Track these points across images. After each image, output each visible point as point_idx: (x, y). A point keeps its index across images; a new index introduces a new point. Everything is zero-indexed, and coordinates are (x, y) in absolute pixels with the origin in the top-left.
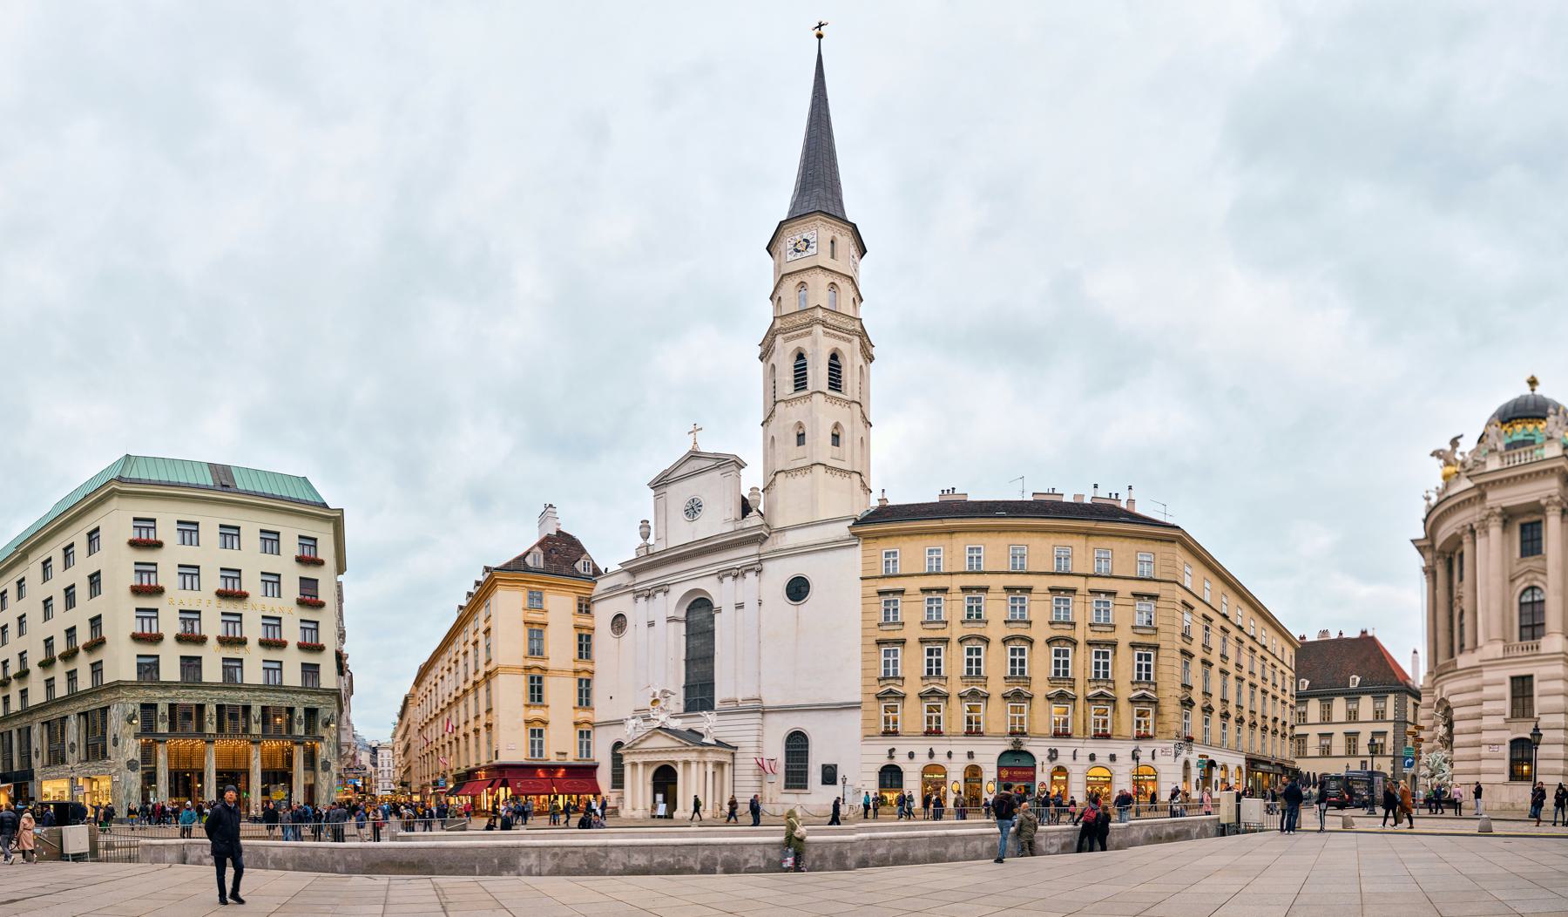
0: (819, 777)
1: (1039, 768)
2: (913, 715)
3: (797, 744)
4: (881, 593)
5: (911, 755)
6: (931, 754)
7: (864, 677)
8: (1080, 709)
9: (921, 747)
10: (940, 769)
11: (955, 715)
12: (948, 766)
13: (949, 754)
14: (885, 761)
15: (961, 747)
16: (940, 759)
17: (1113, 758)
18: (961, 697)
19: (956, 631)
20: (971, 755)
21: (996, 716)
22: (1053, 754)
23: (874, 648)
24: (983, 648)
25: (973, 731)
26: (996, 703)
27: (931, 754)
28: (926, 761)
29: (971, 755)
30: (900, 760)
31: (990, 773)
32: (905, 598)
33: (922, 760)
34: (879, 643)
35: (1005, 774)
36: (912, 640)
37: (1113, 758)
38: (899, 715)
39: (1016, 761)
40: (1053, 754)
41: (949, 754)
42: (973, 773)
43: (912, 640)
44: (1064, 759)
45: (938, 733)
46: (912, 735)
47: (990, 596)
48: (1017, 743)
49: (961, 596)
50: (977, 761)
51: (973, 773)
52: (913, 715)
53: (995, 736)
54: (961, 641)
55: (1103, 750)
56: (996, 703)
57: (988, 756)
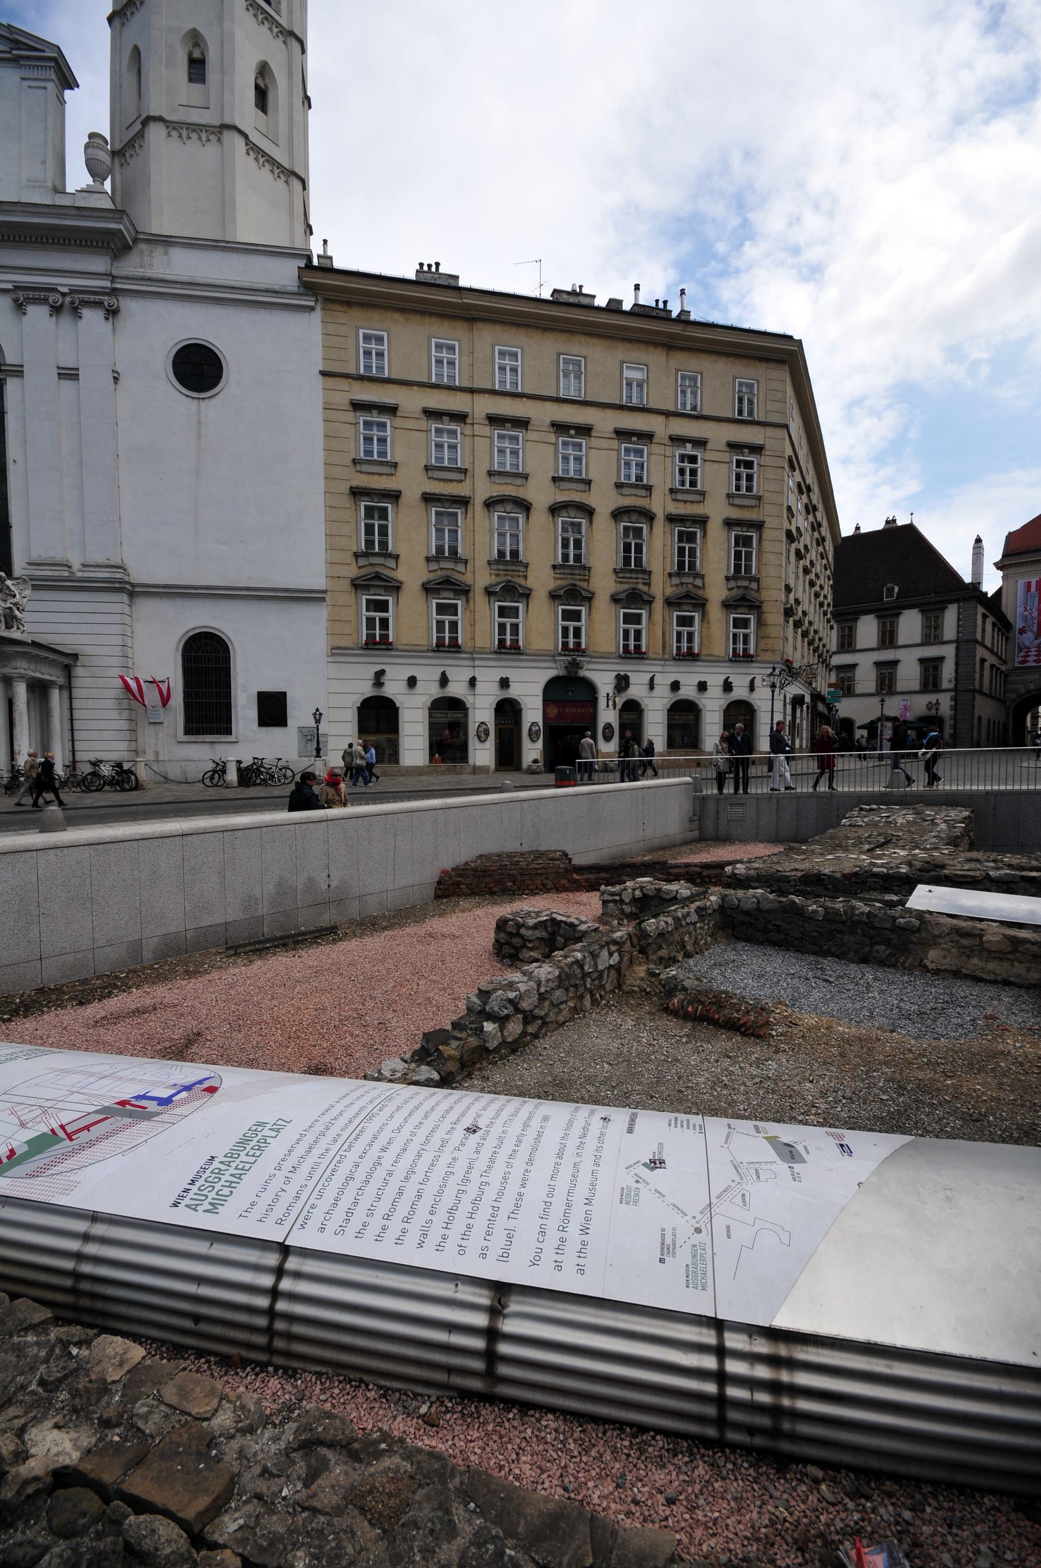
0: (253, 713)
1: (602, 702)
2: (412, 617)
3: (206, 660)
4: (357, 406)
5: (412, 682)
6: (444, 681)
7: (331, 548)
8: (658, 616)
9: (428, 675)
10: (456, 705)
11: (479, 621)
12: (469, 700)
13: (472, 682)
14: (367, 690)
15: (488, 677)
16: (457, 689)
17: (702, 687)
18: (489, 592)
19: (482, 489)
20: (504, 683)
21: (540, 623)
22: (622, 683)
23: (346, 501)
24: (521, 518)
25: (509, 648)
26: (540, 603)
27: (444, 681)
28: (435, 691)
29: (504, 683)
30: (394, 689)
31: (533, 713)
32: (398, 422)
33: (429, 690)
34: (357, 493)
35: (553, 712)
36: (411, 495)
37: (702, 687)
38: (390, 614)
39: (569, 693)
40: (622, 683)
41: (472, 682)
42: (508, 710)
43: (411, 495)
44: (637, 691)
45: (454, 647)
46: (413, 652)
47: (531, 435)
48: (575, 665)
49: (486, 430)
50: (514, 692)
51: (508, 710)
52: (412, 617)
53: (539, 656)
54: (490, 504)
55: (689, 679)
56: (540, 603)
57: (530, 689)
